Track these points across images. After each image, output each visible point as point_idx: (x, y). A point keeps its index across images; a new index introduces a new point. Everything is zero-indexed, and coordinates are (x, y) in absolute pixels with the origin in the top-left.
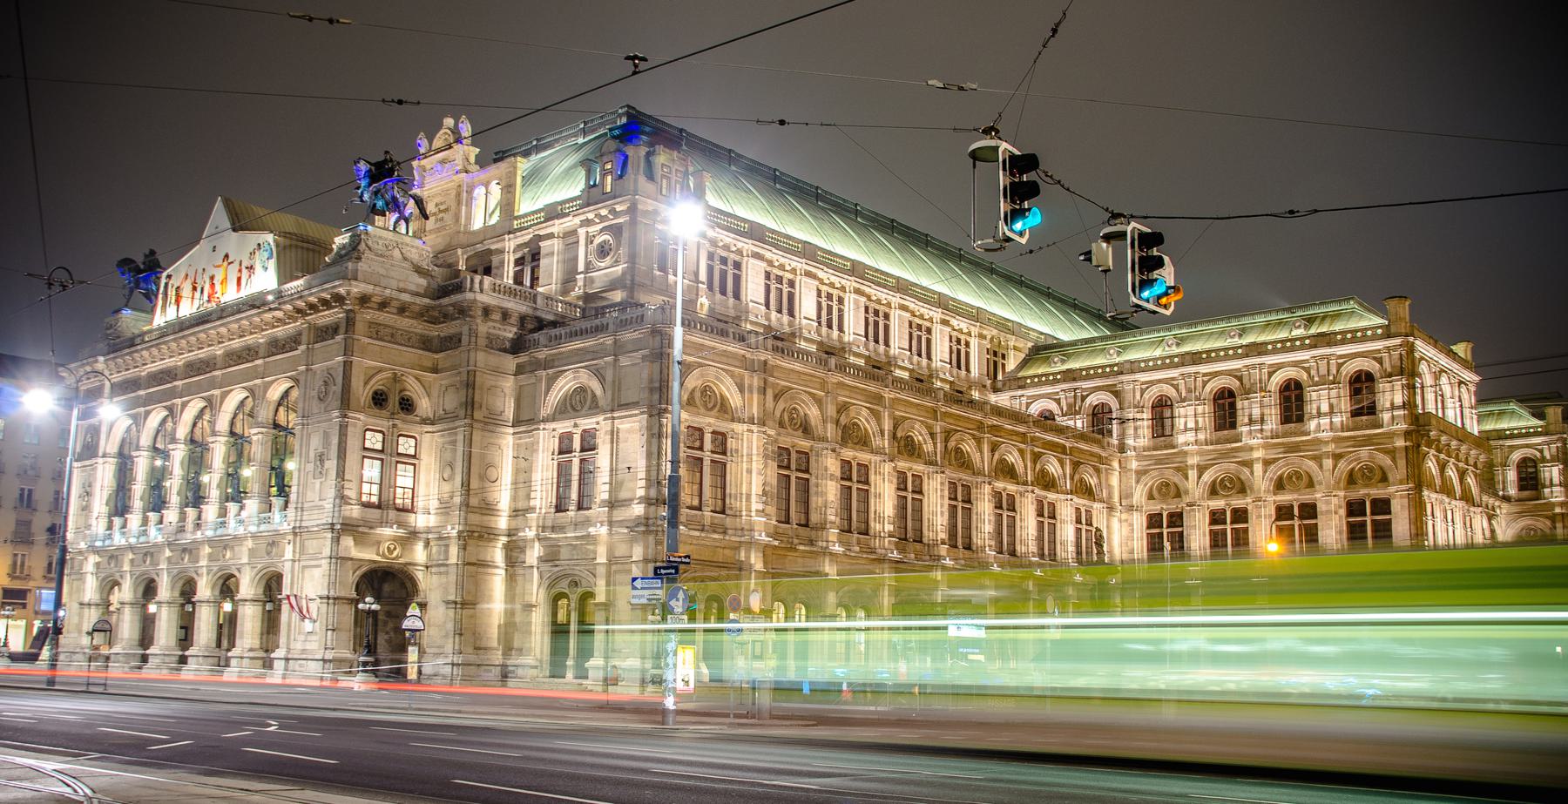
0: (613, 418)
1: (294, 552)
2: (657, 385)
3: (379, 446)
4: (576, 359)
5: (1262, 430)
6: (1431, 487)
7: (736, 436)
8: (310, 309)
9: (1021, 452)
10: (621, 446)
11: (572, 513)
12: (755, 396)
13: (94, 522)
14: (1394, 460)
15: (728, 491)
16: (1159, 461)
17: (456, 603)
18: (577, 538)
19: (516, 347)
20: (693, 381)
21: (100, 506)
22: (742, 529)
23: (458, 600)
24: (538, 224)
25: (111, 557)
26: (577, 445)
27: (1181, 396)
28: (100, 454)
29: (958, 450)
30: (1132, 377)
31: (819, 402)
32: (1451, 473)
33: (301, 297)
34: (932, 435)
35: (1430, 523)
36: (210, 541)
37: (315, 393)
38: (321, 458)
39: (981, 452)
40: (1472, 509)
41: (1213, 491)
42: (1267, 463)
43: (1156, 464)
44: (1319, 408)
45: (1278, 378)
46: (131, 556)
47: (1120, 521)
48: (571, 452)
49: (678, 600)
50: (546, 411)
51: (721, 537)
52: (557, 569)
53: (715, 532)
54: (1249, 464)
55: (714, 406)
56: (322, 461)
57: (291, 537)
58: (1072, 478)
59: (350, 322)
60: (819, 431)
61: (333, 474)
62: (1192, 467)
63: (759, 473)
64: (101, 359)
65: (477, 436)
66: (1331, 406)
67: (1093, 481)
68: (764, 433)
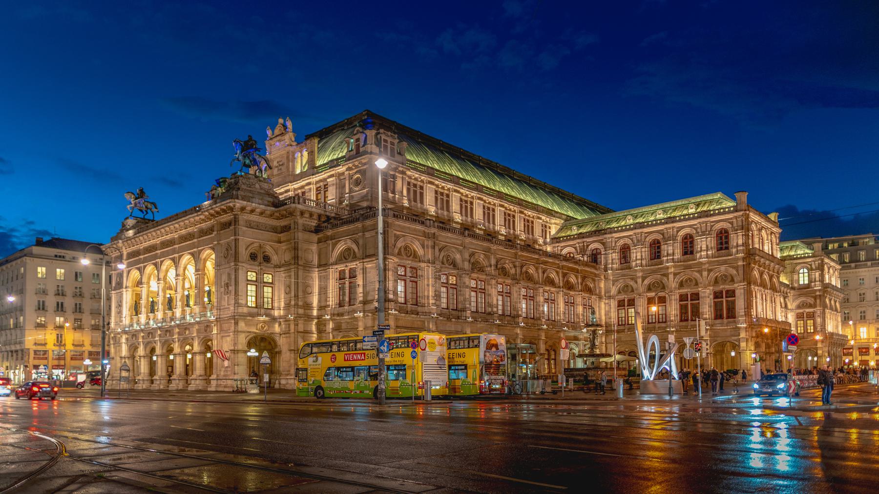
0: (364, 262)
1: (217, 329)
3: (254, 279)
6: (755, 284)
7: (422, 269)
9: (557, 273)
10: (368, 275)
12: (430, 250)
14: (737, 271)
15: (418, 295)
16: (623, 275)
19: (317, 230)
20: (400, 244)
21: (126, 311)
26: (347, 275)
28: (124, 287)
29: (527, 272)
31: (461, 252)
32: (766, 277)
34: (515, 267)
35: (754, 301)
36: (178, 326)
38: (227, 285)
39: (538, 273)
40: (775, 294)
42: (675, 274)
43: (622, 276)
44: (701, 248)
46: (142, 334)
47: (605, 304)
48: (345, 279)
49: (384, 346)
50: (333, 259)
53: (413, 314)
54: (666, 275)
55: (411, 255)
56: (228, 287)
57: (215, 323)
58: (582, 284)
61: (233, 292)
62: (639, 277)
63: (433, 286)
65: (301, 273)
67: (592, 286)
68: (434, 267)
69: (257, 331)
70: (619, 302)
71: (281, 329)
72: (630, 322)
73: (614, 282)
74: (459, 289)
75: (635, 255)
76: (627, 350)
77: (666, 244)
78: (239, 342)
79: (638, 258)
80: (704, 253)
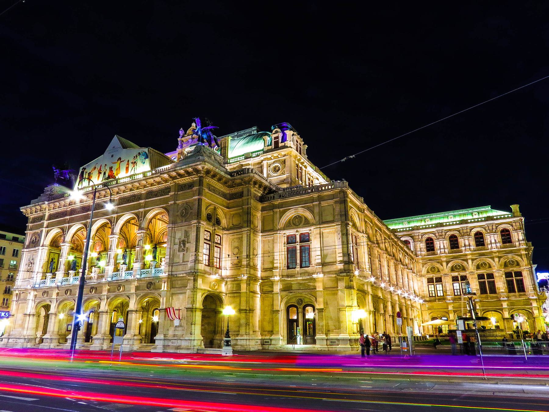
2: (343, 213)
4: (295, 204)
8: (179, 176)
10: (324, 239)
11: (298, 269)
16: (430, 260)
17: (246, 310)
18: (303, 280)
19: (262, 199)
22: (365, 277)
23: (248, 309)
24: (234, 162)
25: (45, 292)
27: (437, 238)
28: (41, 245)
30: (418, 231)
33: (175, 170)
37: (179, 213)
41: (453, 269)
43: (429, 261)
45: (474, 231)
48: (296, 243)
52: (291, 294)
54: (466, 260)
59: (200, 182)
62: (444, 261)
64: (46, 203)
66: (495, 240)
69: (210, 289)
70: (428, 279)
71: (227, 289)
72: (439, 295)
73: (424, 264)
74: (372, 258)
75: (438, 246)
76: (439, 316)
77: (463, 238)
79: (442, 247)
80: (494, 245)
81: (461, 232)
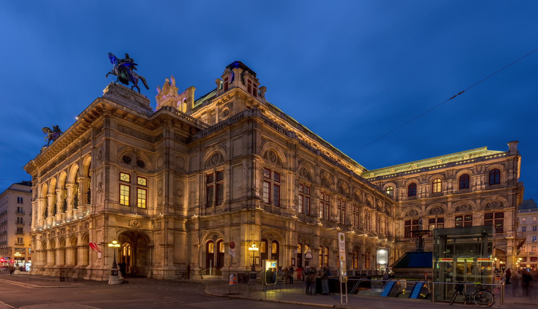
5: (452, 192)
7: (284, 176)
9: (372, 197)
13: (38, 222)
20: (266, 148)
21: (40, 216)
27: (420, 182)
29: (355, 194)
31: (314, 167)
34: (349, 188)
46: (48, 233)
51: (279, 216)
53: (275, 213)
55: (275, 161)
60: (314, 179)
63: (293, 191)
69: (130, 227)
71: (154, 227)
75: (420, 190)
78: (109, 235)
79: (423, 191)
81: (446, 175)
